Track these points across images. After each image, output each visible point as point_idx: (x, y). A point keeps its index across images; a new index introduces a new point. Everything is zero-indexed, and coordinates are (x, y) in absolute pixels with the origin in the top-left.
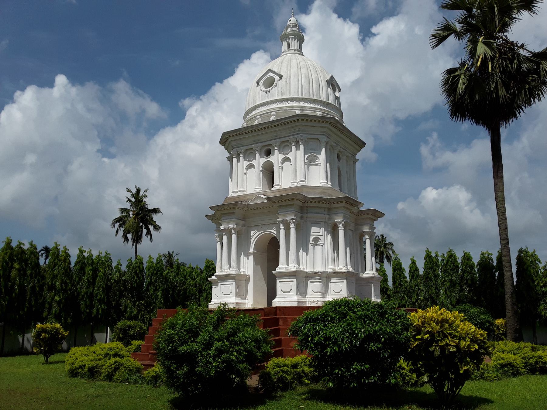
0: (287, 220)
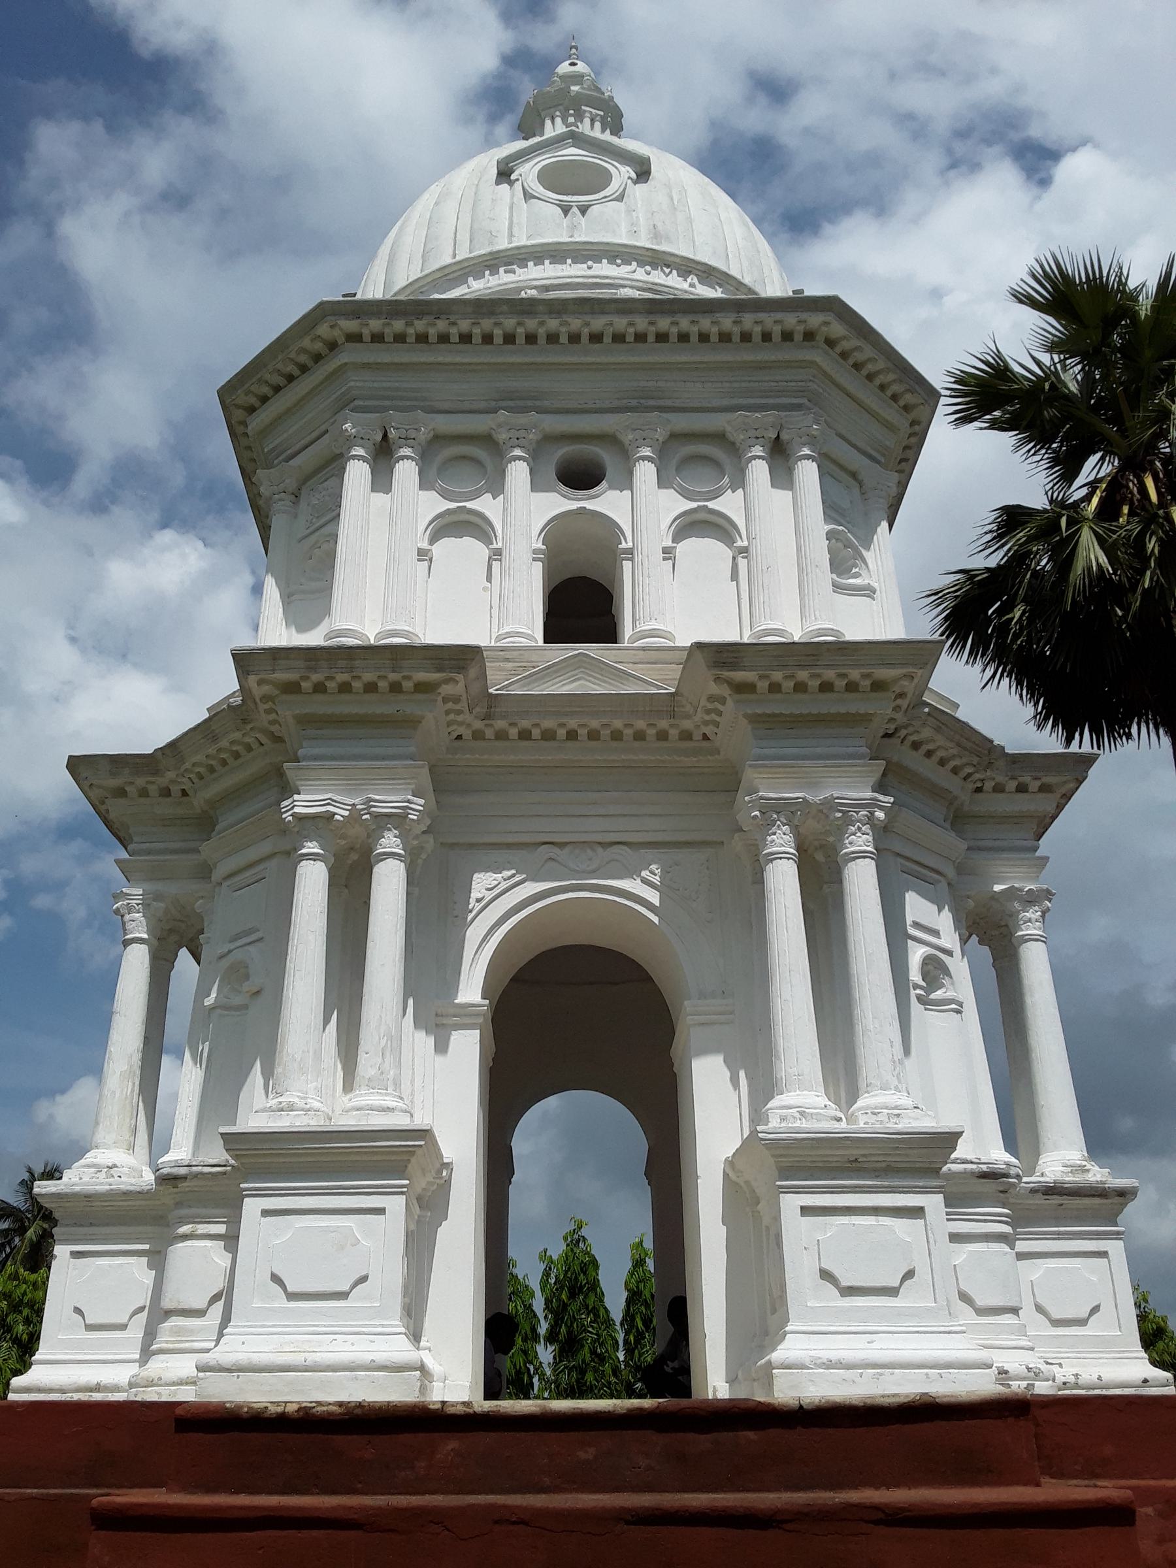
0: (830, 804)
